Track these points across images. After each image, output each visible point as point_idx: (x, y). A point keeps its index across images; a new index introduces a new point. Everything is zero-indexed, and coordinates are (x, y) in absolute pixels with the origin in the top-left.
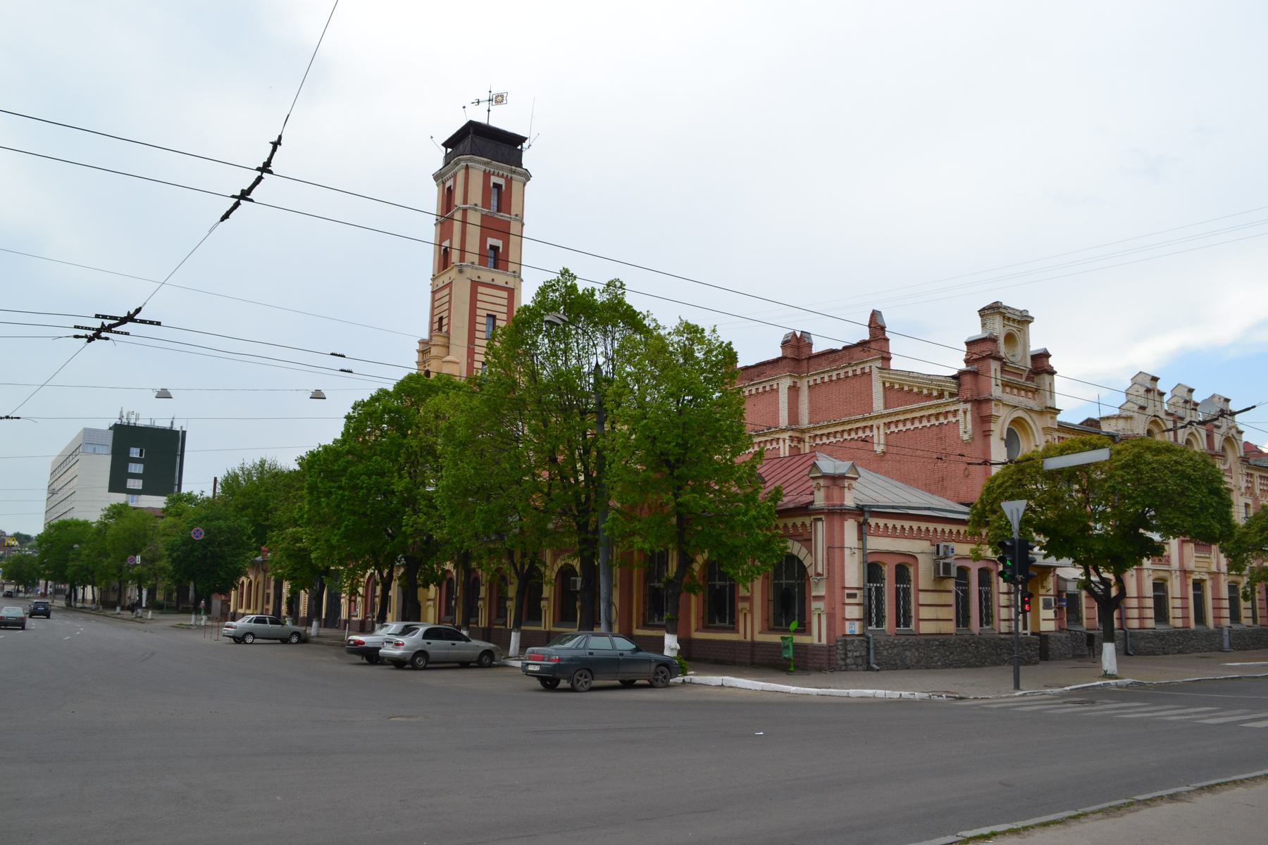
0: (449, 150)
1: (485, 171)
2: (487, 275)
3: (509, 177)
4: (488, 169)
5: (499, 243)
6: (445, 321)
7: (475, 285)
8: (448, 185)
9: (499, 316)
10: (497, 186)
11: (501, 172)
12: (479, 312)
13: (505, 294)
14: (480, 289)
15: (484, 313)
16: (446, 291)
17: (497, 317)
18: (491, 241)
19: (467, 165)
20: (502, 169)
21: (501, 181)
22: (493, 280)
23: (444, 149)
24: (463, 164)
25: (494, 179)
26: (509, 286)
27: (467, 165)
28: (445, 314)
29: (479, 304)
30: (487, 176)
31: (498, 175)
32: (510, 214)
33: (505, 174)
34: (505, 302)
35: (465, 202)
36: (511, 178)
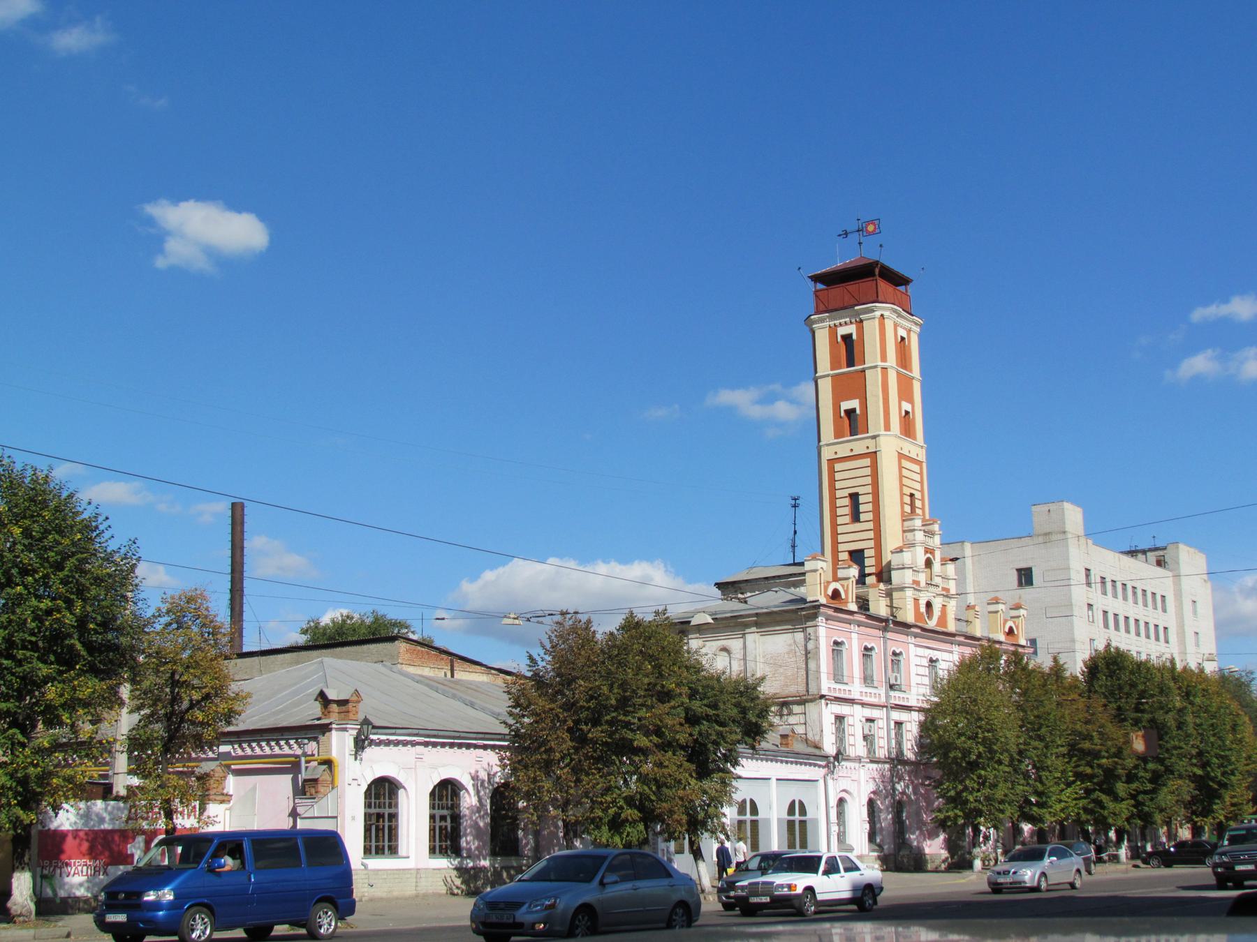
0: (820, 286)
6: (862, 499)
7: (901, 456)
8: (842, 331)
9: (918, 495)
13: (916, 468)
14: (905, 463)
16: (867, 462)
19: (882, 315)
21: (904, 334)
23: (811, 284)
24: (878, 314)
25: (902, 333)
27: (882, 315)
28: (860, 490)
30: (896, 326)
32: (911, 371)
35: (884, 359)
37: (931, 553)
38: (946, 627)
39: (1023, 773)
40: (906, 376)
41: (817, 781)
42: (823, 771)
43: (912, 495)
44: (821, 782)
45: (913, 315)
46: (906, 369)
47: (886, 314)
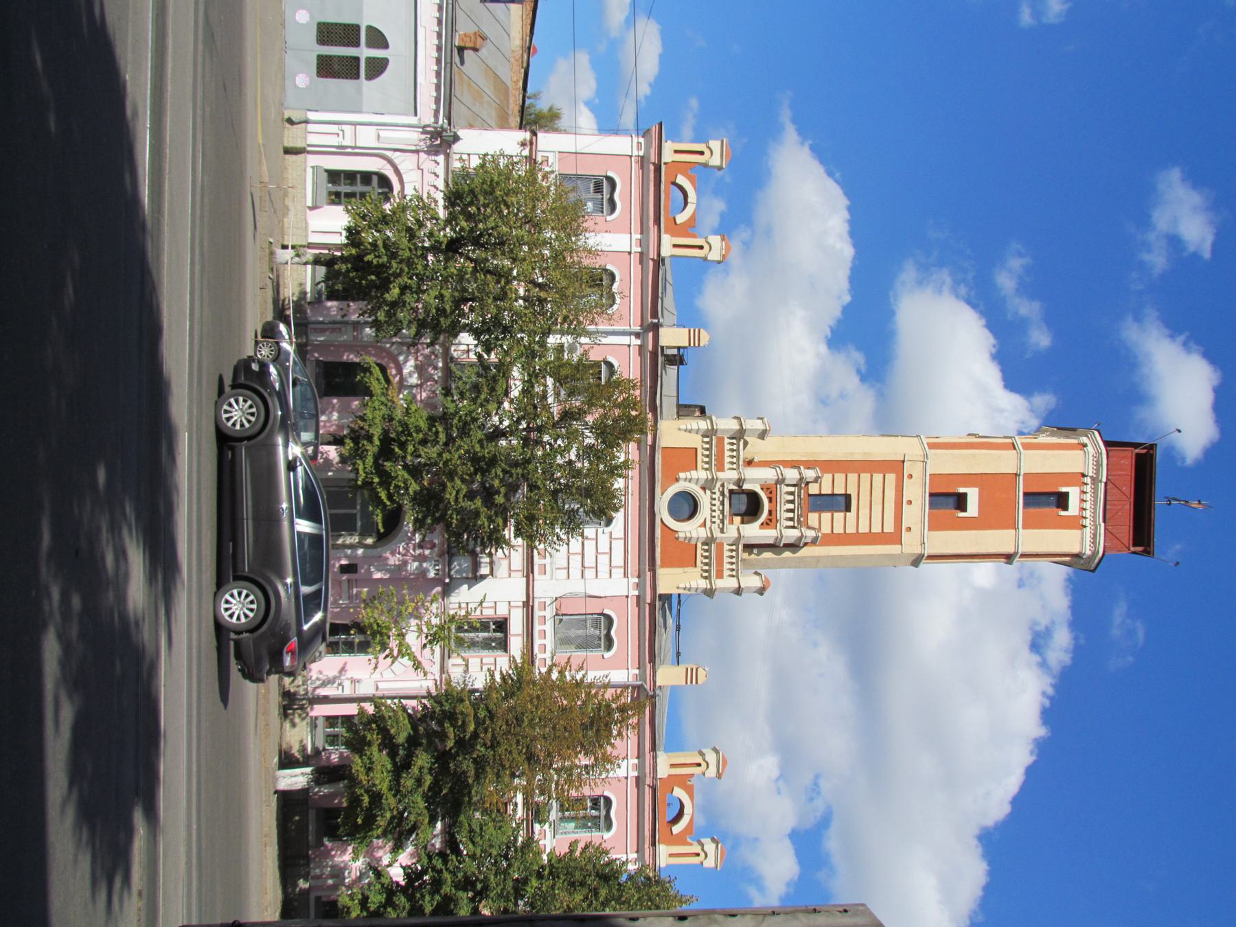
1: (1083, 475)
2: (917, 493)
3: (1084, 522)
4: (1087, 480)
5: (973, 509)
7: (896, 467)
9: (851, 516)
10: (1062, 501)
11: (1088, 505)
12: (853, 477)
13: (889, 528)
14: (891, 478)
15: (852, 491)
17: (848, 514)
18: (973, 495)
19: (1085, 445)
20: (1095, 502)
22: (910, 502)
25: (1074, 493)
26: (905, 536)
29: (865, 477)
30: (1078, 478)
31: (1083, 501)
33: (1088, 514)
34: (876, 529)
36: (1085, 527)
37: (770, 512)
38: (662, 566)
39: (443, 519)
40: (1016, 503)
41: (416, 114)
42: (429, 120)
43: (846, 503)
44: (413, 120)
45: (1104, 521)
46: (1024, 508)
47: (1090, 448)
